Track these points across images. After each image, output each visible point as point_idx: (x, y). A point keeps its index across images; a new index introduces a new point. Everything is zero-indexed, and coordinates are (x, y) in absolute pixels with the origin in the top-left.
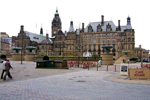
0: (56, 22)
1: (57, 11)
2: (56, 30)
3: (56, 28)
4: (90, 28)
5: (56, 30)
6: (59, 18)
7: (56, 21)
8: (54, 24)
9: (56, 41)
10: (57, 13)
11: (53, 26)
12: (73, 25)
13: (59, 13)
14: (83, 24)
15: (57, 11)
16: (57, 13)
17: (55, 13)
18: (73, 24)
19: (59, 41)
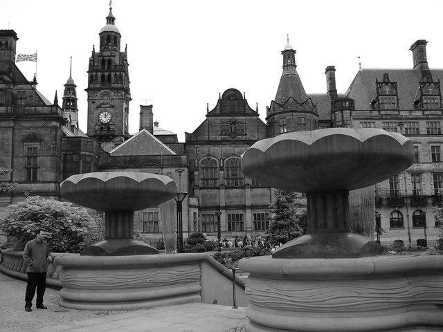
0: (109, 68)
1: (111, 19)
2: (113, 107)
3: (112, 93)
4: (387, 89)
5: (113, 107)
6: (122, 50)
7: (110, 62)
8: (103, 76)
9: (206, 149)
10: (110, 27)
11: (99, 86)
12: (295, 66)
13: (119, 26)
14: (330, 70)
15: (111, 19)
16: (111, 26)
17: (102, 24)
18: (294, 62)
19: (228, 149)
